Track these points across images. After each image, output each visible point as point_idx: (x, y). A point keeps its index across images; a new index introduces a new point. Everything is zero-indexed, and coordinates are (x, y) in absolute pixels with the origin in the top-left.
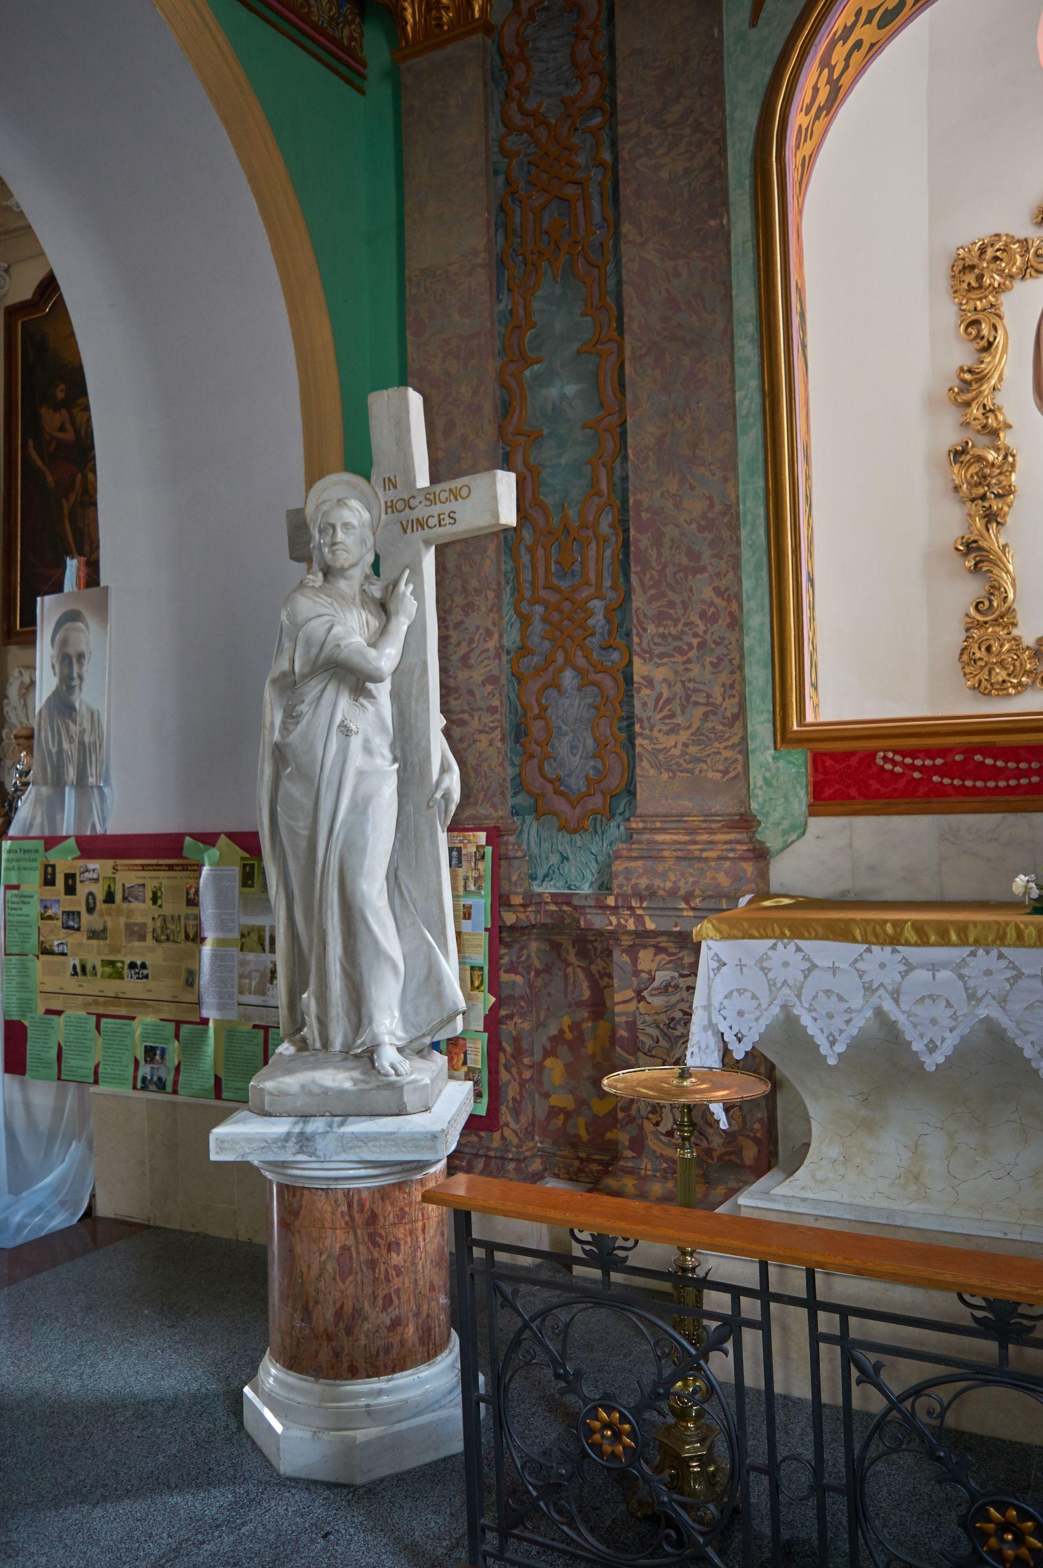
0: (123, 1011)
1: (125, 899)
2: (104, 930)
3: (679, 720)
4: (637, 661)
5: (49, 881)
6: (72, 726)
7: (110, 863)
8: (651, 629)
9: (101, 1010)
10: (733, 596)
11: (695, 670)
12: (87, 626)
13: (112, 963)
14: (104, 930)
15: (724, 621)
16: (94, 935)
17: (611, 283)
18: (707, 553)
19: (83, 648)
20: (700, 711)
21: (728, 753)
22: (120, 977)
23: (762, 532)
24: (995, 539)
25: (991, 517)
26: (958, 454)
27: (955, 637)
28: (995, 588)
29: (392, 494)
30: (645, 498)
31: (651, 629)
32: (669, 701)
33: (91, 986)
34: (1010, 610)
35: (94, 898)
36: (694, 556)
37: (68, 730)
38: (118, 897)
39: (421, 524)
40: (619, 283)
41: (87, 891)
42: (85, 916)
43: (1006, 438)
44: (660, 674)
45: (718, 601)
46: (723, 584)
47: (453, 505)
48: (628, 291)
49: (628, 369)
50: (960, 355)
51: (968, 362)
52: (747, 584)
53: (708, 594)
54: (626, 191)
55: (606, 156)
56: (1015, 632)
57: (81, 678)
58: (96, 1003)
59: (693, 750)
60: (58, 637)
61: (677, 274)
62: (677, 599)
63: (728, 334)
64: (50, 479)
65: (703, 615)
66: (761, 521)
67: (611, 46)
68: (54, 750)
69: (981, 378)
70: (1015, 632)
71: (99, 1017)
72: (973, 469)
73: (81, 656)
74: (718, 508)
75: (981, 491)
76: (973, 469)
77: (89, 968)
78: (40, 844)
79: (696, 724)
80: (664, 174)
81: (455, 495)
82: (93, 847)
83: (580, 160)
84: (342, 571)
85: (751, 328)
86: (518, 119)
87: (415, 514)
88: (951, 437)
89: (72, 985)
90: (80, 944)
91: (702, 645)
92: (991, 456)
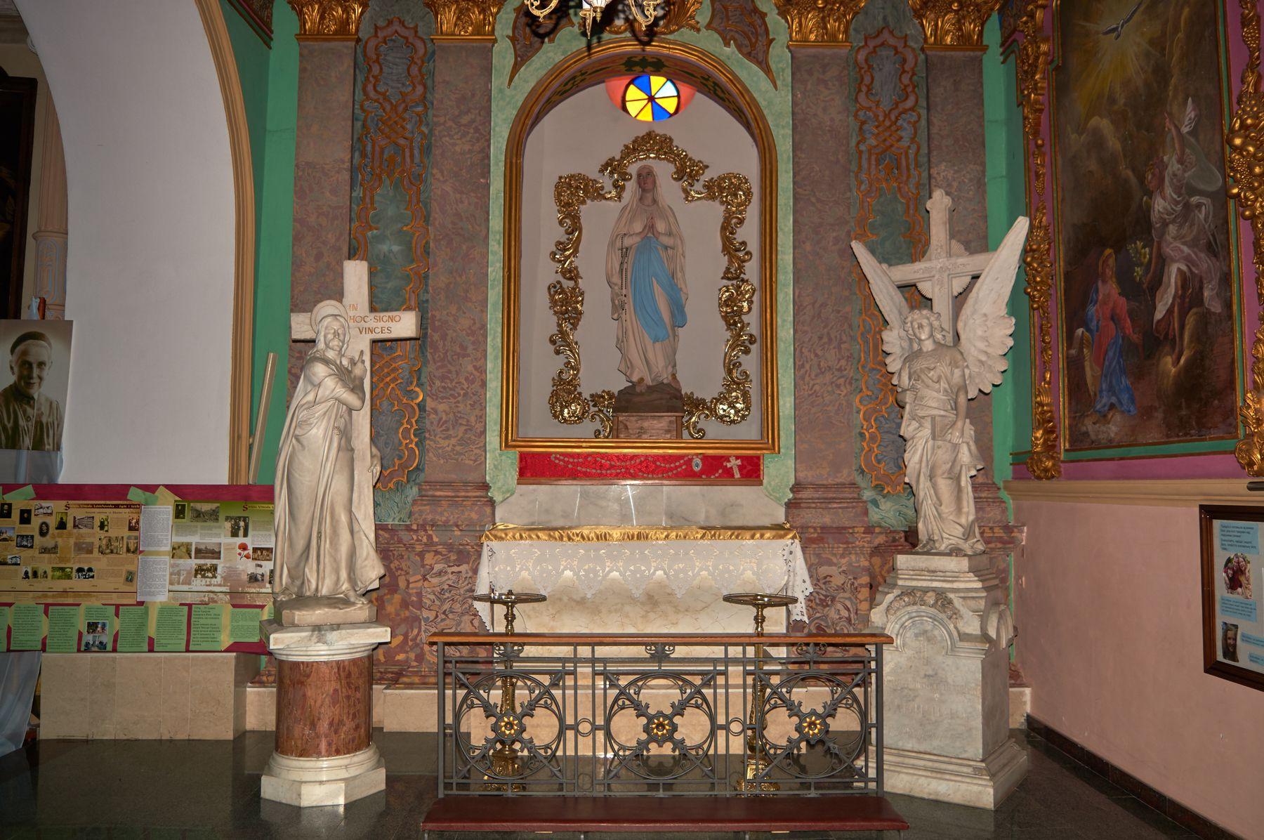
0: (70, 601)
1: (75, 526)
2: (56, 547)
3: (451, 432)
6: (29, 409)
7: (64, 503)
8: (438, 383)
9: (50, 601)
10: (483, 371)
11: (461, 406)
12: (50, 344)
13: (63, 569)
14: (56, 547)
16: (45, 550)
19: (45, 358)
20: (464, 428)
21: (478, 451)
22: (69, 577)
23: (499, 340)
30: (437, 314)
31: (438, 383)
32: (446, 422)
33: (41, 585)
35: (47, 526)
36: (463, 348)
37: (25, 412)
38: (70, 525)
39: (371, 331)
41: (40, 521)
42: (38, 539)
44: (441, 407)
45: (475, 373)
46: (479, 364)
50: (559, 234)
52: (489, 366)
53: (470, 368)
57: (40, 378)
58: (46, 596)
59: (458, 448)
60: (20, 348)
61: (462, 202)
62: (453, 369)
65: (467, 379)
66: (500, 335)
68: (9, 426)
71: (47, 606)
73: (41, 364)
74: (478, 325)
77: (40, 572)
79: (461, 435)
80: (458, 149)
85: (499, 237)
86: (372, 94)
87: (367, 325)
89: (24, 585)
90: (33, 557)
91: (465, 395)
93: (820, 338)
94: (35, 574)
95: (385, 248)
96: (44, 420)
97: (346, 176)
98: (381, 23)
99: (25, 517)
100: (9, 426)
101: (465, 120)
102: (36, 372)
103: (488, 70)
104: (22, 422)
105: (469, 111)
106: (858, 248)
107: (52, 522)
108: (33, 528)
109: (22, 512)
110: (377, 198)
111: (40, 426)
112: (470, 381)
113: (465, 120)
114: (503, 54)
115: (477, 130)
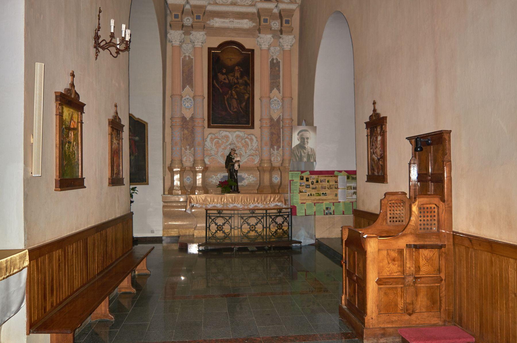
5: (302, 178)
16: (313, 188)
19: (308, 137)
22: (320, 195)
33: (312, 198)
38: (319, 182)
57: (308, 142)
64: (221, 90)
68: (299, 155)
71: (315, 203)
73: (307, 138)
78: (300, 172)
82: (313, 173)
94: (311, 195)
96: (310, 153)
99: (307, 180)
100: (299, 155)
102: (306, 140)
104: (303, 154)
107: (315, 181)
108: (310, 182)
109: (307, 178)
111: (308, 155)
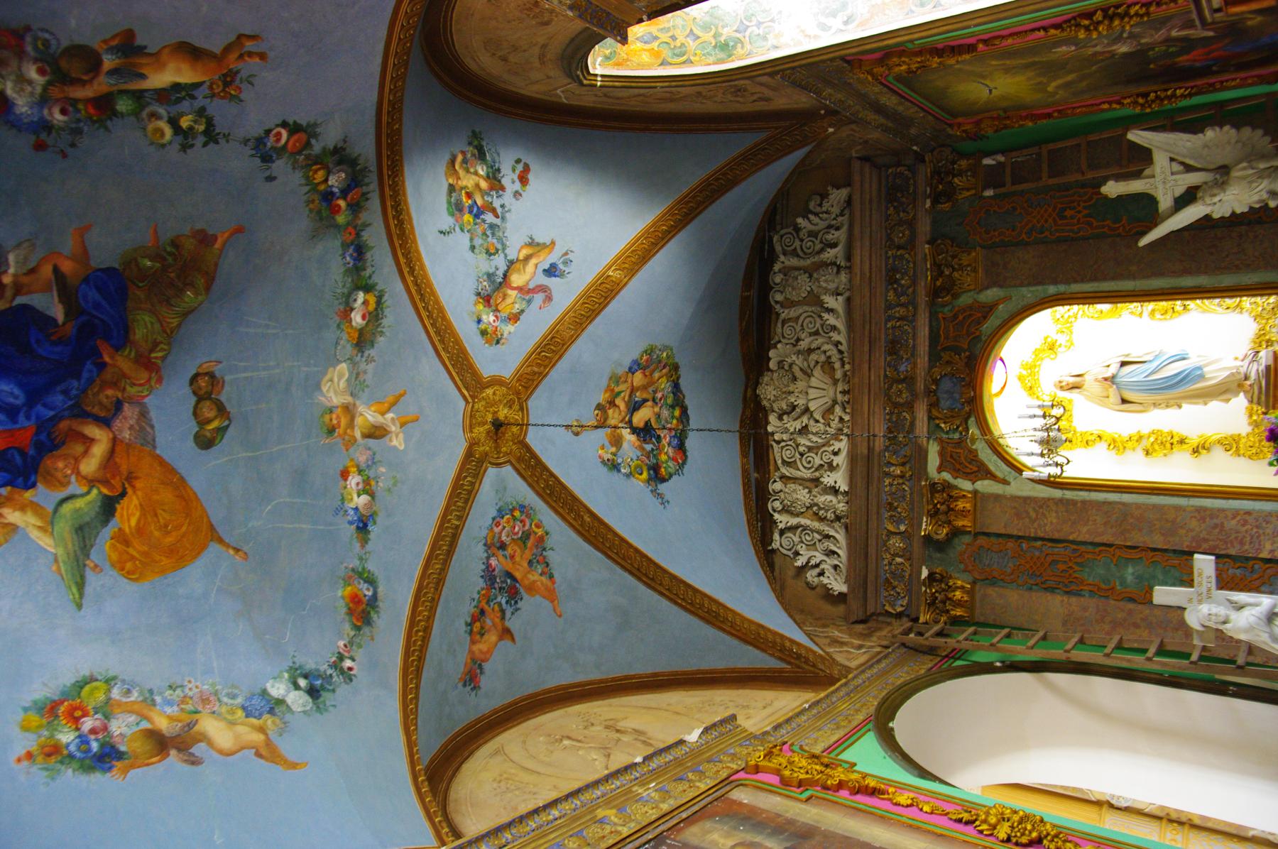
4: (1261, 556)
8: (1246, 547)
10: (1236, 513)
15: (1247, 517)
17: (1090, 548)
18: (1215, 521)
24: (1194, 441)
25: (1182, 442)
26: (1147, 453)
27: (1243, 462)
28: (1219, 442)
29: (1195, 600)
30: (1186, 543)
31: (1246, 547)
34: (1231, 436)
36: (1216, 526)
39: (1209, 590)
40: (1092, 544)
43: (1145, 432)
44: (1268, 546)
47: (1204, 575)
48: (1098, 540)
49: (1129, 544)
50: (1102, 446)
51: (1106, 446)
53: (1234, 522)
54: (1056, 536)
55: (1039, 543)
56: (1244, 434)
62: (1234, 536)
63: (1124, 504)
65: (1243, 525)
67: (999, 535)
69: (1114, 441)
70: (1244, 434)
72: (1156, 447)
75: (1168, 445)
76: (1156, 447)
81: (1200, 575)
83: (1037, 553)
84: (1227, 616)
88: (1140, 453)
91: (1257, 527)
92: (1152, 439)
93: (1212, 254)
95: (1129, 578)
97: (1074, 600)
98: (962, 566)
101: (1033, 515)
103: (997, 497)
105: (1028, 513)
106: (1144, 241)
110: (1090, 581)
112: (1245, 523)
113: (1033, 515)
114: (984, 486)
115: (1041, 507)
